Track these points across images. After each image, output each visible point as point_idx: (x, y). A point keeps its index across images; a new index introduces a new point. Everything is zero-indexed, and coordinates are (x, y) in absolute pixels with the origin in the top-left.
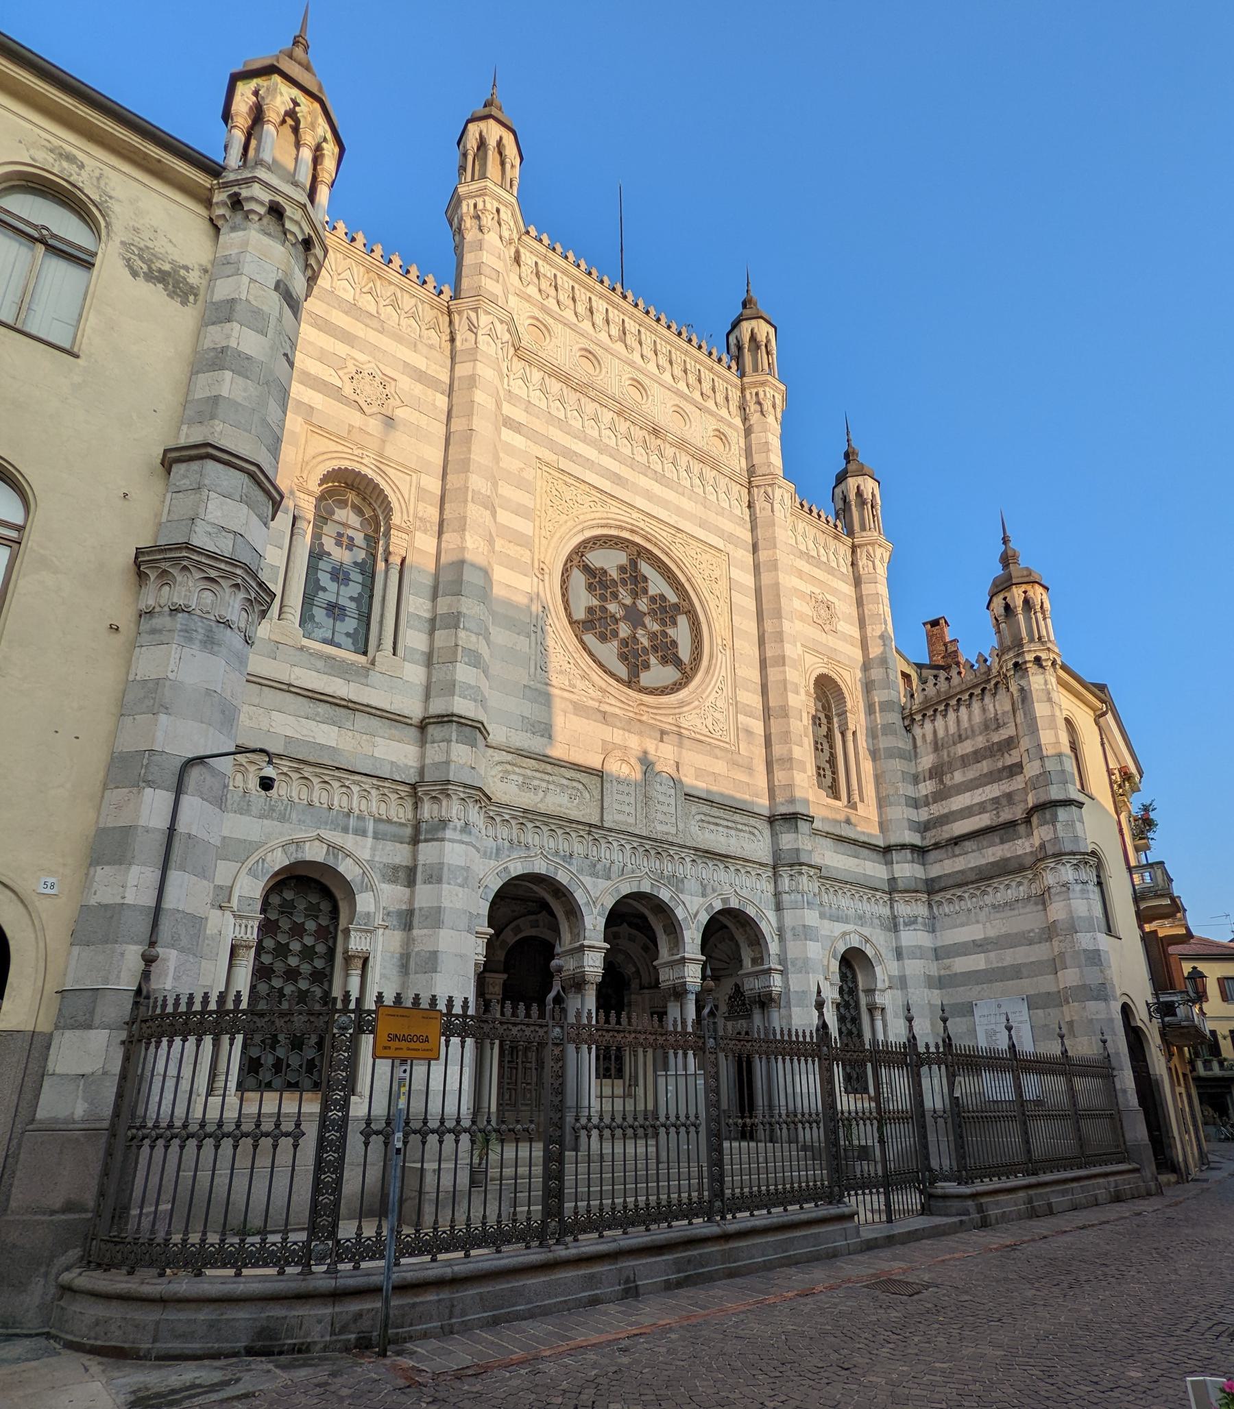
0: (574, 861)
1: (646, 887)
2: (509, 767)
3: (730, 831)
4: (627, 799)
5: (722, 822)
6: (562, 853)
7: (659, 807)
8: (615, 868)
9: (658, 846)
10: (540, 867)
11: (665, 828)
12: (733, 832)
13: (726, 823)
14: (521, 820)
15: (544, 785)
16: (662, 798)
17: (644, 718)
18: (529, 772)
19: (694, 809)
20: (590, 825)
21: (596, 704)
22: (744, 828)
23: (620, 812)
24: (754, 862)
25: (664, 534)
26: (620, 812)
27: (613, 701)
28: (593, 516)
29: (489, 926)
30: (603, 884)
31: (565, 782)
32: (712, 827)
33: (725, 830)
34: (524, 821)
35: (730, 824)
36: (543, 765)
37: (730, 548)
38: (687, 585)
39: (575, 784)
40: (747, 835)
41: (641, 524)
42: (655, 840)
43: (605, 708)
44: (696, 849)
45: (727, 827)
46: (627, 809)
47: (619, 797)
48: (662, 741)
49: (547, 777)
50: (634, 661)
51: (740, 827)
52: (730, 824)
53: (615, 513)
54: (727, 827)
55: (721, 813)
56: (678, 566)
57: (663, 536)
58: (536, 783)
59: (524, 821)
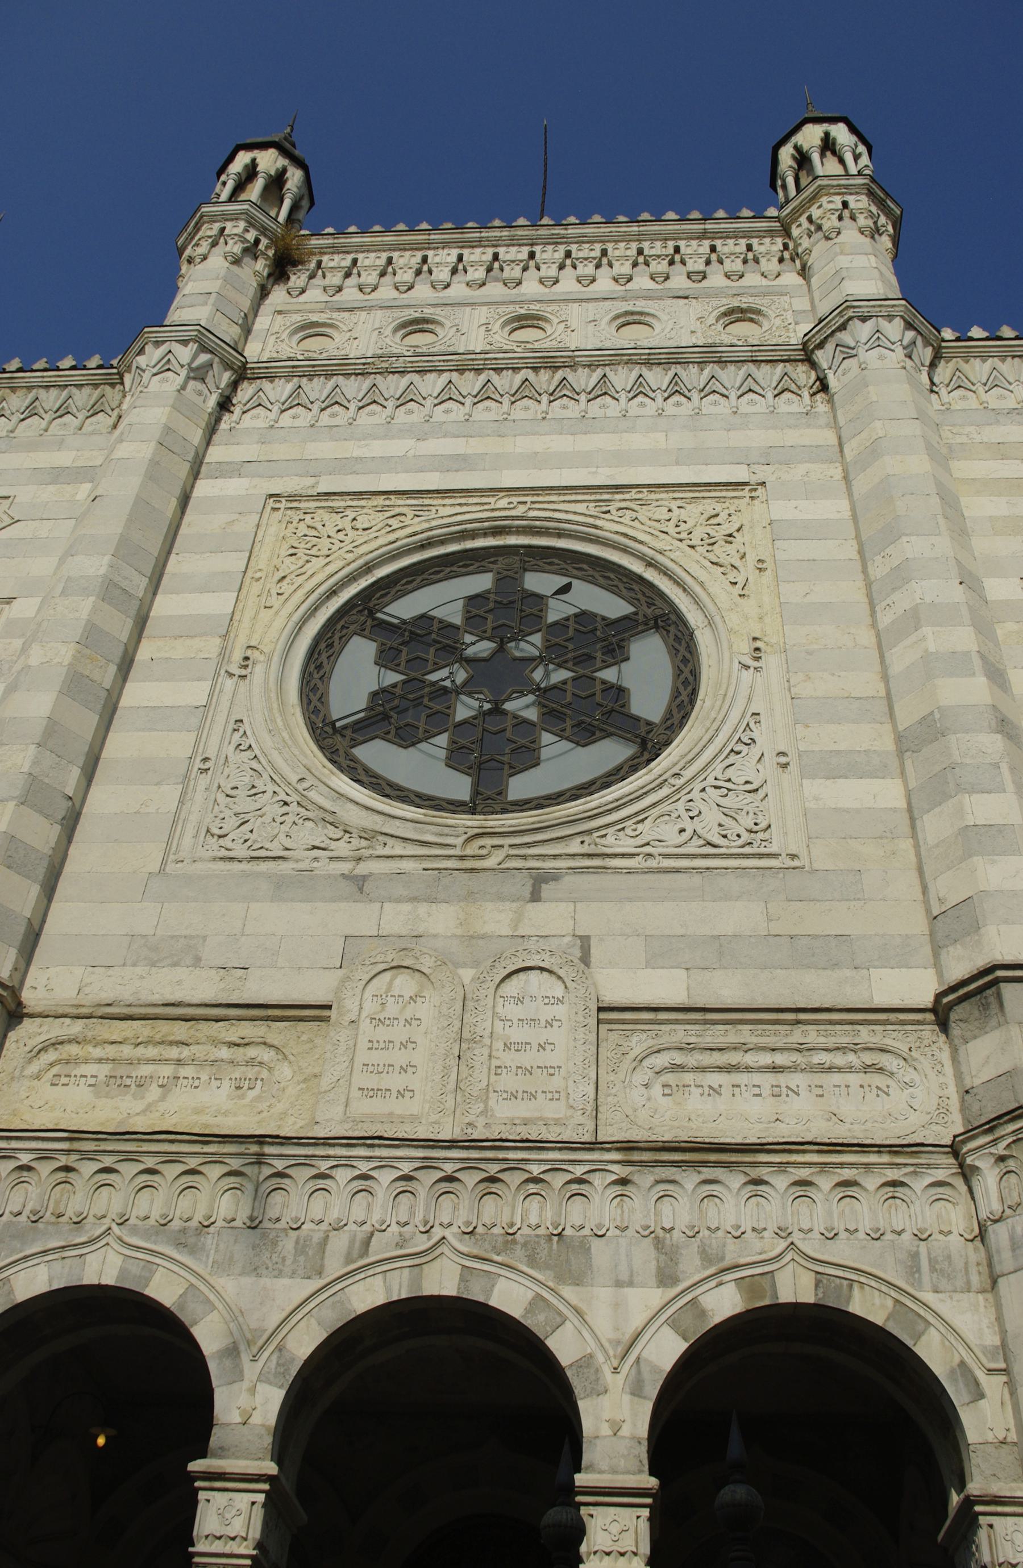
0: (209, 1241)
1: (442, 1281)
2: (74, 1049)
3: (782, 1079)
4: (399, 1057)
5: (750, 1059)
6: (176, 1224)
7: (510, 1059)
8: (339, 1243)
9: (491, 1158)
10: (103, 1268)
11: (522, 1110)
12: (796, 1080)
13: (766, 1059)
14: (63, 1160)
15: (167, 1071)
16: (517, 1034)
17: (491, 862)
18: (127, 1051)
19: (638, 1042)
20: (261, 1139)
21: (345, 867)
22: (838, 1059)
23: (370, 1093)
24: (863, 1147)
25: (581, 508)
26: (370, 1093)
27: (399, 849)
28: (392, 537)
30: (292, 1290)
31: (224, 1053)
32: (715, 1079)
33: (767, 1080)
34: (71, 1160)
35: (780, 1059)
36: (164, 1028)
37: (763, 473)
38: (650, 575)
39: (252, 1052)
40: (854, 1079)
41: (520, 511)
42: (473, 1144)
43: (362, 869)
44: (628, 1147)
45: (775, 1069)
46: (395, 1081)
47: (376, 1057)
48: (535, 897)
49: (174, 1052)
50: (491, 763)
51: (818, 1058)
52: (780, 1059)
53: (444, 514)
54: (775, 1069)
55: (745, 1034)
56: (624, 550)
57: (577, 511)
58: (145, 1070)
59: (71, 1160)
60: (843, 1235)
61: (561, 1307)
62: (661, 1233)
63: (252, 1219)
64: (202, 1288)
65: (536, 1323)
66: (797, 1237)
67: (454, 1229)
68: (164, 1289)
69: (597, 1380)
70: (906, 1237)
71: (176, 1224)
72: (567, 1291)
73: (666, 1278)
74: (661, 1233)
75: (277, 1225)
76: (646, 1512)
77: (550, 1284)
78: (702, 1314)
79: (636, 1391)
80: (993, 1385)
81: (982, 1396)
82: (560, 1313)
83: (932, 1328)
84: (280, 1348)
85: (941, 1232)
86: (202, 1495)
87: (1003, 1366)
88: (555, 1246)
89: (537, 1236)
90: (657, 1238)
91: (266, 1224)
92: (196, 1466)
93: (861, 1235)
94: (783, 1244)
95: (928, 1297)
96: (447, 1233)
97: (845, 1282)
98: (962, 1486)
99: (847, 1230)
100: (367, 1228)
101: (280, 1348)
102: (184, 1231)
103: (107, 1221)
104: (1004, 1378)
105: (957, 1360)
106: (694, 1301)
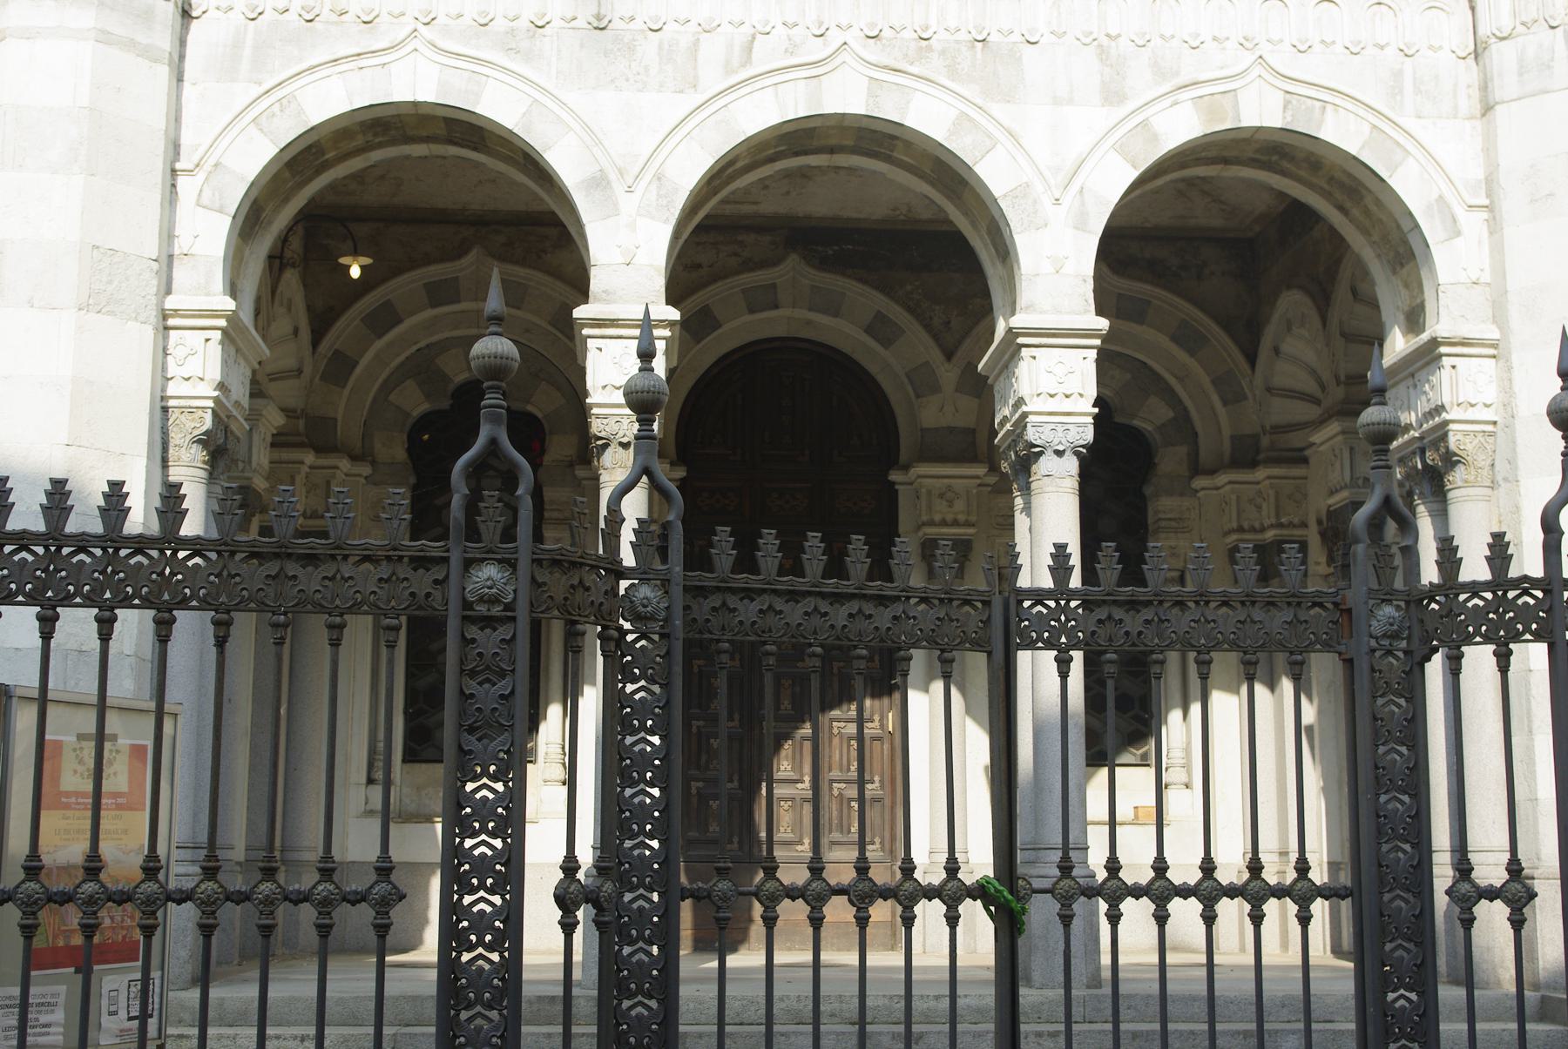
29: (1100, 312)
60: (1318, 48)
61: (991, 128)
62: (1105, 41)
63: (599, 18)
64: (549, 103)
65: (962, 146)
66: (1265, 49)
67: (855, 32)
68: (499, 105)
69: (1036, 212)
70: (1391, 51)
71: (500, 25)
72: (996, 109)
73: (1112, 95)
74: (1105, 41)
75: (632, 25)
76: (1093, 354)
77: (979, 101)
78: (1155, 138)
79: (1081, 225)
80: (1473, 224)
81: (1459, 234)
82: (990, 136)
83: (1411, 160)
84: (659, 177)
85: (1431, 47)
86: (591, 343)
87: (1486, 202)
88: (979, 55)
89: (957, 42)
90: (1100, 46)
91: (617, 24)
92: (579, 312)
93: (1339, 48)
94: (1249, 58)
95: (1409, 122)
96: (853, 37)
97: (1318, 104)
98: (1414, 320)
99: (1323, 42)
100: (746, 30)
101: (659, 177)
102: (512, 32)
103: (408, 19)
104: (1485, 215)
105: (1435, 196)
106: (1145, 124)
